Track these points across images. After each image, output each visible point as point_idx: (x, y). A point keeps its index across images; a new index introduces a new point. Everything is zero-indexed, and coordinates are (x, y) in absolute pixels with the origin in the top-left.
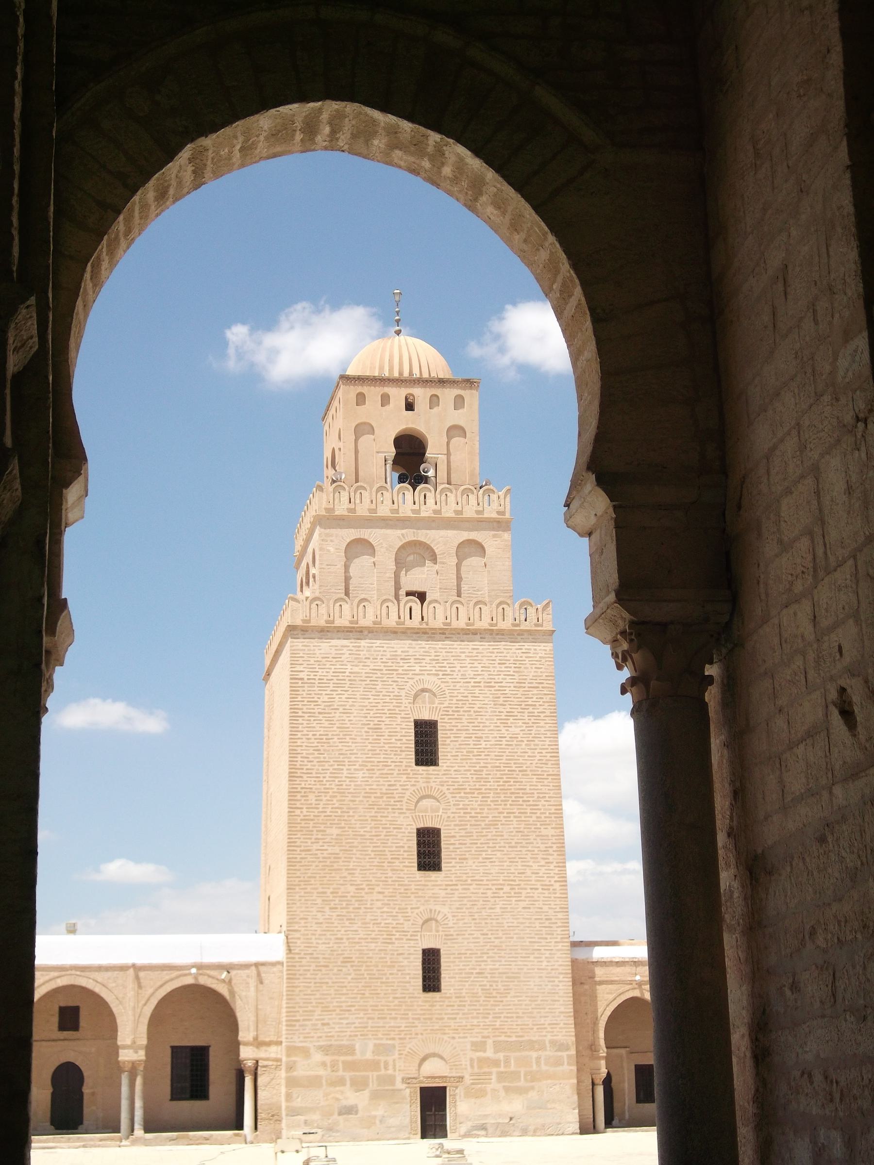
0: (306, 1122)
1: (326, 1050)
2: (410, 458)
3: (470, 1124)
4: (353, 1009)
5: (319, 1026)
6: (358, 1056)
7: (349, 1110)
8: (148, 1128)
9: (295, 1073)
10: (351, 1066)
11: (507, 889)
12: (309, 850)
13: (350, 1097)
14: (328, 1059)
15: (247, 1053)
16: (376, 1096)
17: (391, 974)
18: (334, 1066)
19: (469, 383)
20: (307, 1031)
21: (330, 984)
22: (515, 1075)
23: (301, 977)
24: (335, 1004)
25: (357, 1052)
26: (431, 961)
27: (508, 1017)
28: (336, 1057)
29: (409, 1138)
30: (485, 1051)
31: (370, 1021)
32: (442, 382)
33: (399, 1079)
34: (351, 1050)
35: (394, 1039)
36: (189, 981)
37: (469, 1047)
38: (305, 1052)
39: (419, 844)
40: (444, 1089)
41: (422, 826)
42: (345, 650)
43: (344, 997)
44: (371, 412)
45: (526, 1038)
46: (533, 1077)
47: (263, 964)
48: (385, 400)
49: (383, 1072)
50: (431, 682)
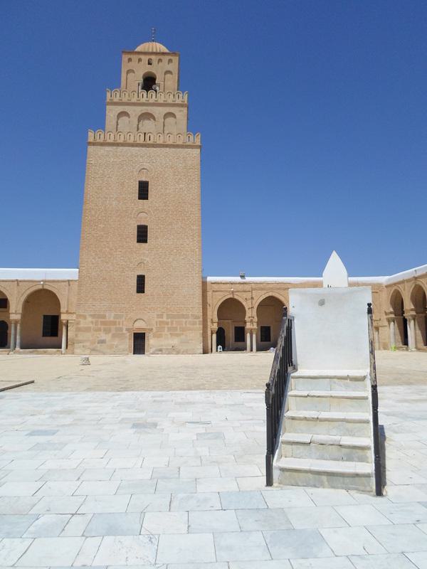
0: (83, 346)
1: (93, 316)
2: (149, 83)
3: (154, 349)
6: (107, 320)
7: (103, 342)
8: (22, 347)
9: (79, 326)
10: (103, 323)
11: (175, 251)
13: (103, 336)
14: (94, 320)
15: (63, 317)
16: (114, 336)
18: (96, 323)
19: (174, 54)
22: (175, 329)
26: (141, 282)
32: (164, 54)
33: (124, 328)
34: (104, 317)
36: (41, 287)
38: (85, 317)
39: (138, 232)
40: (145, 333)
41: (139, 224)
42: (111, 153)
44: (134, 65)
46: (183, 330)
47: (72, 281)
48: (140, 60)
49: (118, 326)
50: (146, 165)
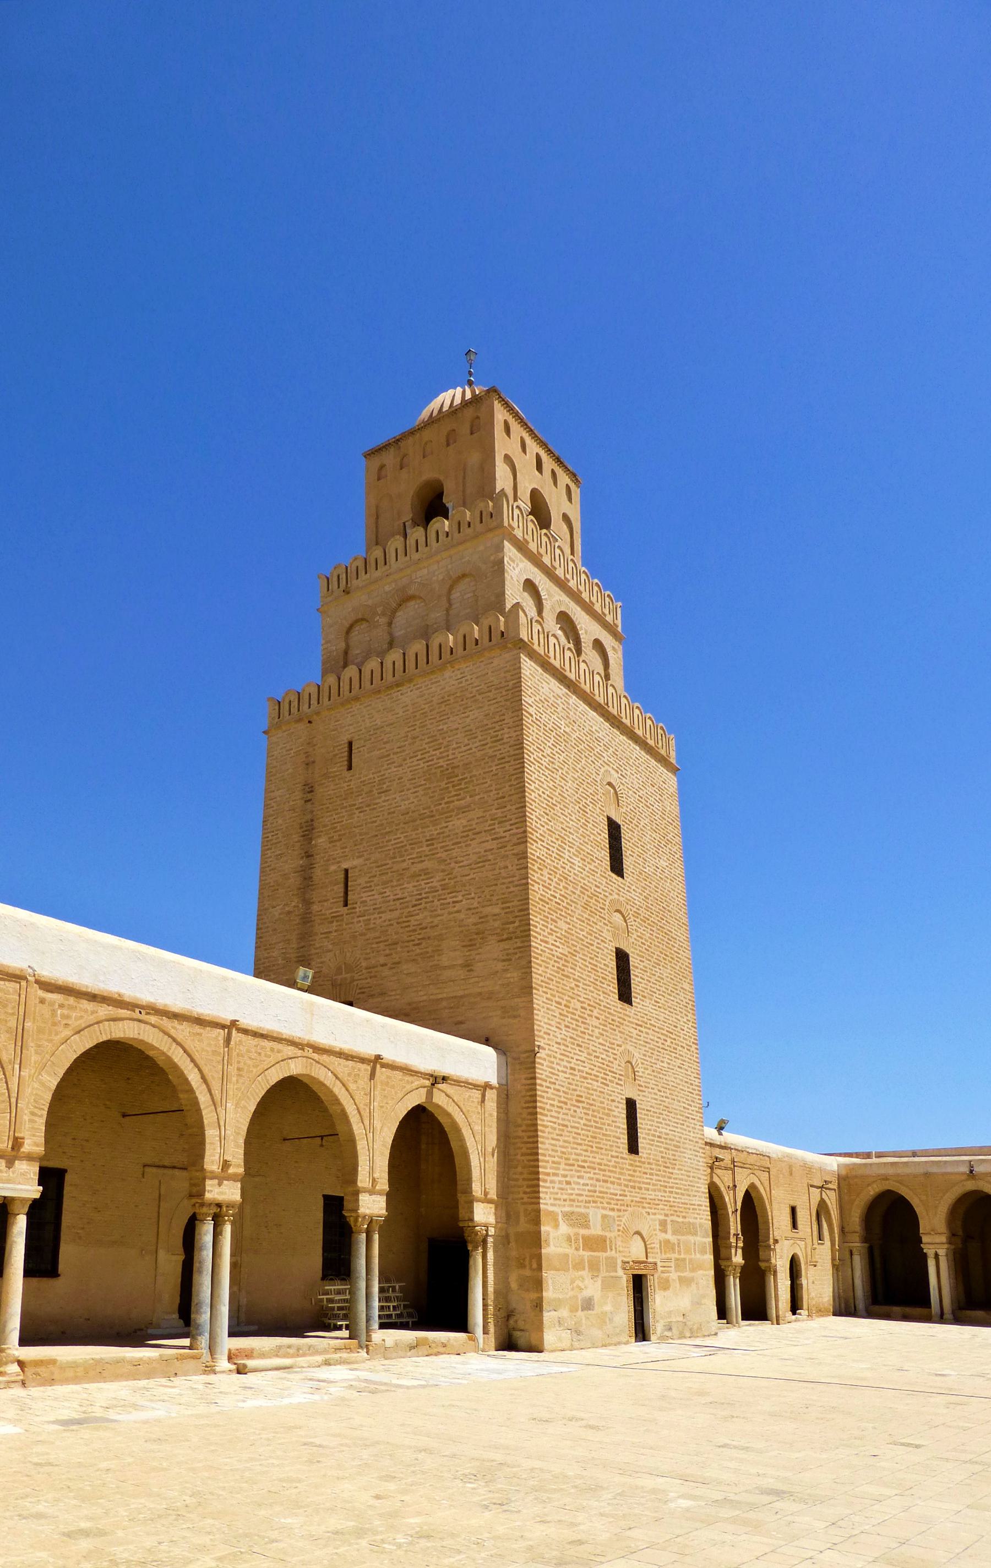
4: (586, 1165)
5: (564, 1186)
7: (588, 1305)
11: (669, 1040)
12: (546, 942)
17: (609, 1125)
20: (556, 1190)
21: (569, 1129)
23: (549, 1113)
24: (574, 1156)
25: (591, 1223)
27: (677, 1193)
28: (576, 1230)
29: (627, 1343)
30: (666, 1232)
31: (598, 1183)
35: (613, 1210)
37: (658, 1227)
43: (579, 1147)
45: (687, 1220)
50: (614, 778)
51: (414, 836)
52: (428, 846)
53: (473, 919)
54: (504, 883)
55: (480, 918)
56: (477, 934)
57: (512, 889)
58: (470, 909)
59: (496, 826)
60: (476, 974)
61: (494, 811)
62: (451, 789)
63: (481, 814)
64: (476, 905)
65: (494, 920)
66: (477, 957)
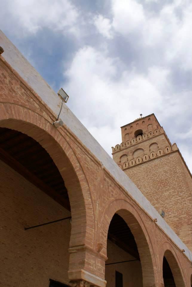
51: (151, 199)
52: (156, 201)
53: (176, 219)
54: (185, 208)
55: (179, 218)
56: (179, 223)
57: (189, 209)
58: (175, 216)
59: (180, 193)
60: (181, 236)
61: (178, 189)
62: (162, 185)
63: (173, 191)
64: (176, 215)
65: (184, 219)
66: (180, 230)
